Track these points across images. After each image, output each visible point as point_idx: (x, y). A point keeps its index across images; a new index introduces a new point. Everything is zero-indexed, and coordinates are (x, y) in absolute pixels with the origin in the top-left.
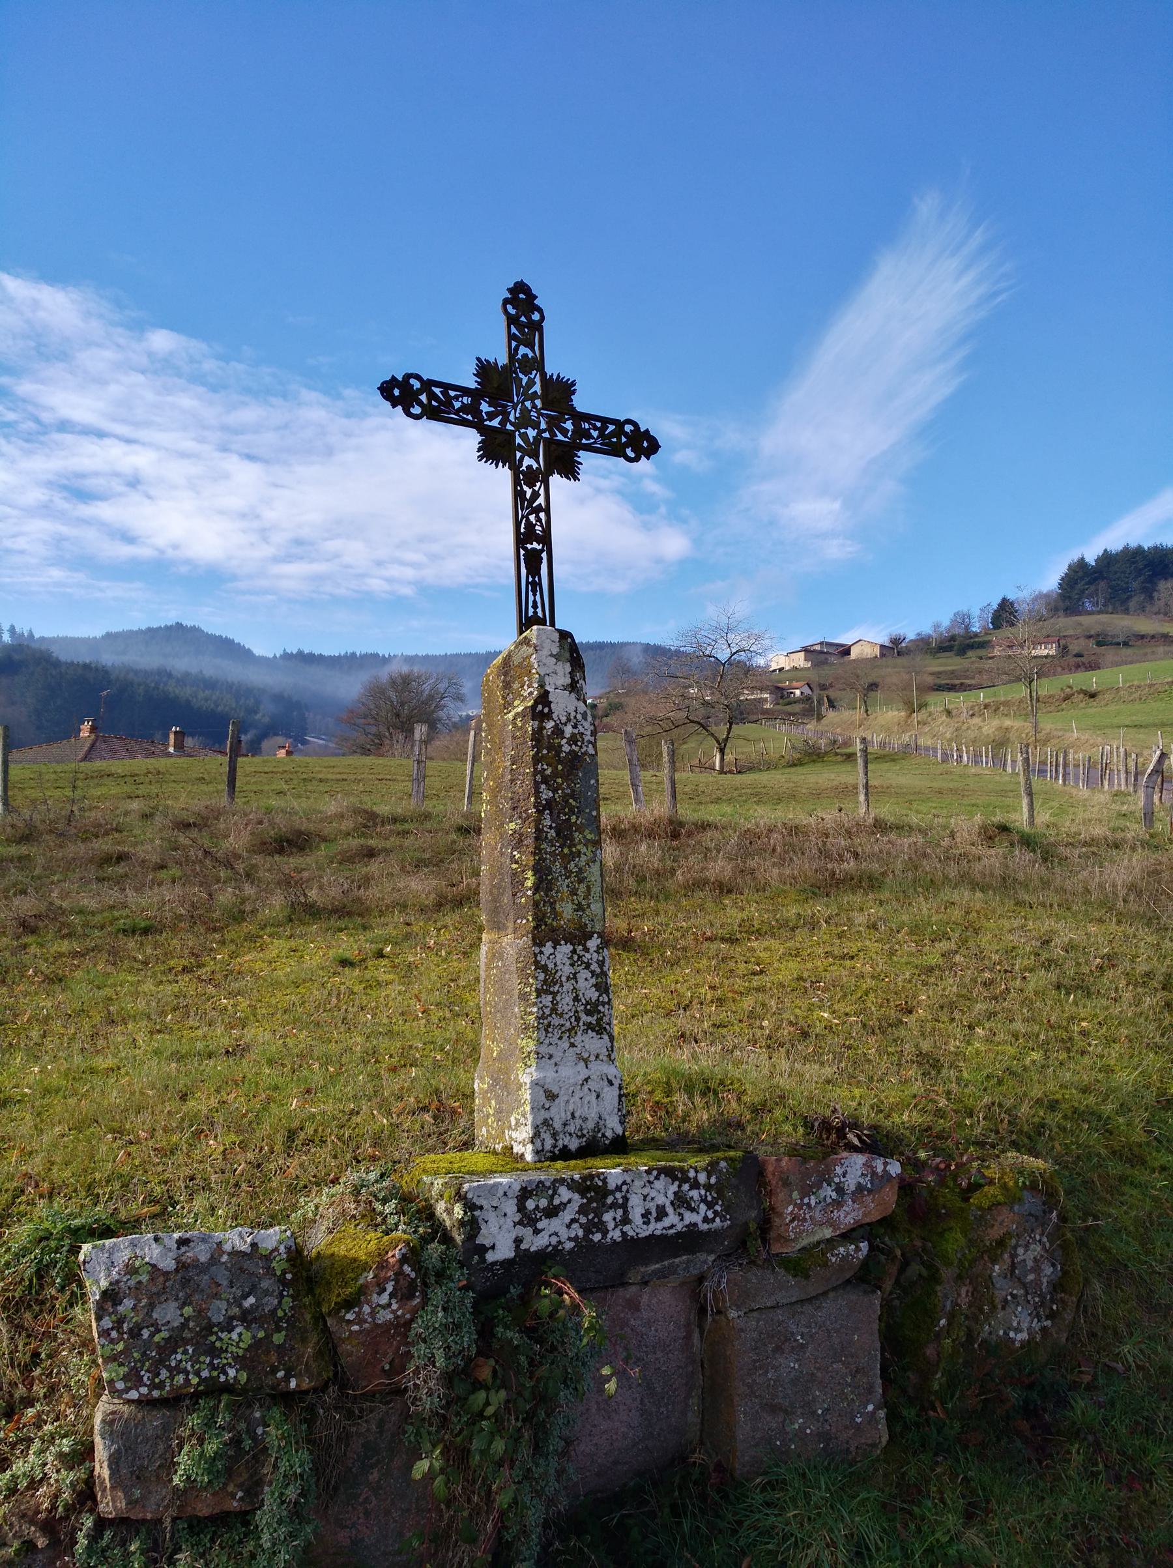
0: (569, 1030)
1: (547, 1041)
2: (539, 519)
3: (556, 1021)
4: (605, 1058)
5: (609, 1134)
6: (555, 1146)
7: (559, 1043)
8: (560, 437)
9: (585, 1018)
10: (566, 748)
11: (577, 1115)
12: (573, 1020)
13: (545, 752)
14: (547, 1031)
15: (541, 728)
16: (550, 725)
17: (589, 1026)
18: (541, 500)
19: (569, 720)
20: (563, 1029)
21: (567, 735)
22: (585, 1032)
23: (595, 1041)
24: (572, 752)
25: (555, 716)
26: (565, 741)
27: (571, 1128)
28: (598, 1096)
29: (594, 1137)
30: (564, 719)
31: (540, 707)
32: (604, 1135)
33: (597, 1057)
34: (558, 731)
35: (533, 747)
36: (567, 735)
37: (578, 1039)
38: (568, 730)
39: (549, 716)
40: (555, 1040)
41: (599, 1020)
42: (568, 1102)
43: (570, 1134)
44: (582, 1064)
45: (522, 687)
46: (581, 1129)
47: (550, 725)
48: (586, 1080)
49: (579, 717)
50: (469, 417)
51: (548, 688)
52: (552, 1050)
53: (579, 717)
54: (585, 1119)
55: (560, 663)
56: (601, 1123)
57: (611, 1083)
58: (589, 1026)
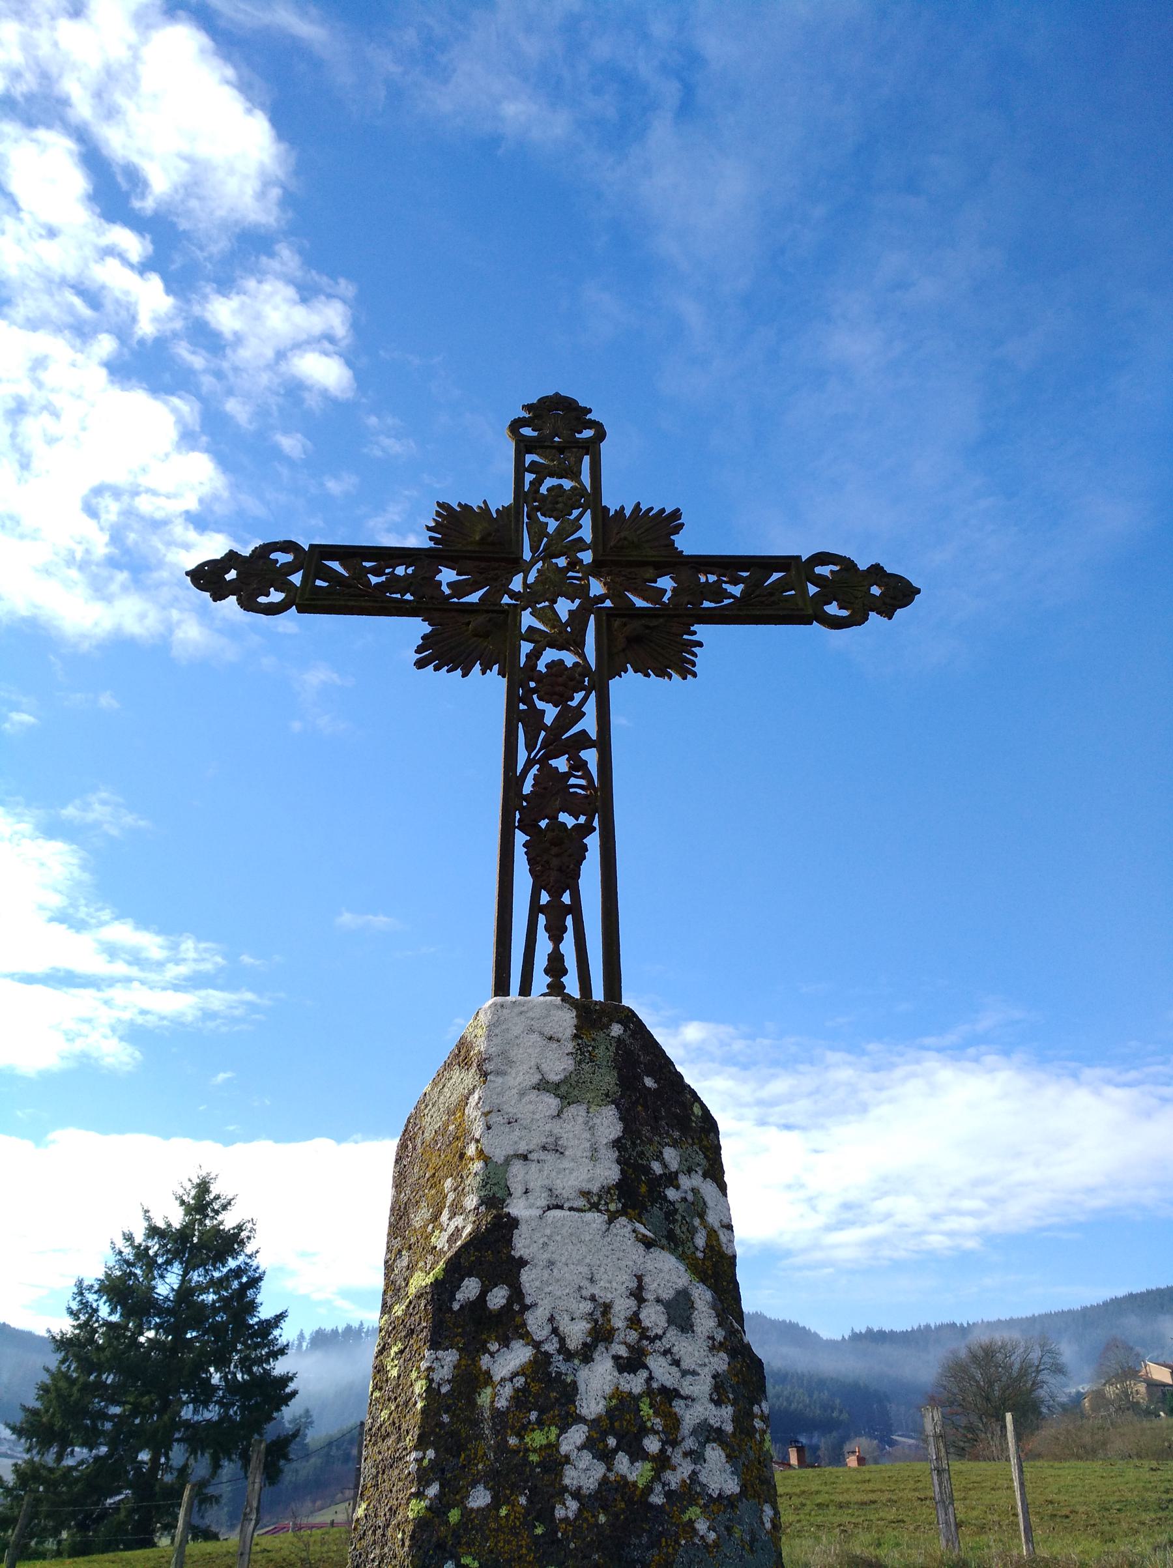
2: (579, 765)
8: (639, 603)
10: (584, 1473)
13: (480, 1498)
15: (471, 1379)
16: (508, 1362)
18: (589, 724)
19: (601, 1334)
21: (592, 1405)
24: (612, 1491)
25: (536, 1322)
26: (577, 1435)
30: (576, 1332)
31: (470, 1288)
34: (548, 1392)
35: (423, 1477)
36: (592, 1405)
38: (597, 1383)
39: (509, 1324)
45: (436, 1217)
47: (508, 1362)
49: (653, 1317)
50: (408, 597)
51: (517, 1208)
53: (653, 1317)
55: (576, 1112)
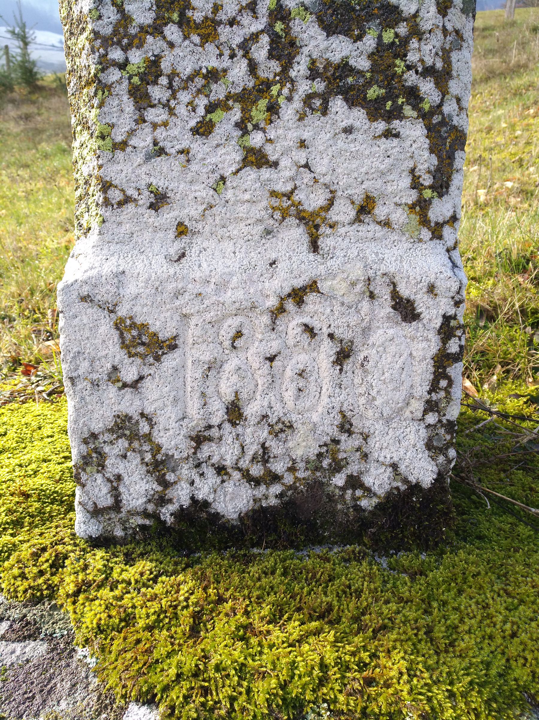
0: (246, 98)
1: (143, 140)
3: (184, 56)
4: (399, 216)
5: (378, 480)
6: (162, 500)
7: (198, 147)
9: (316, 43)
11: (252, 410)
12: (261, 51)
14: (140, 97)
17: (338, 80)
20: (219, 91)
22: (316, 105)
23: (360, 143)
27: (226, 452)
28: (343, 356)
29: (316, 486)
32: (354, 482)
33: (365, 209)
37: (283, 134)
40: (178, 134)
41: (388, 55)
42: (213, 367)
43: (221, 470)
44: (295, 234)
46: (264, 455)
48: (298, 295)
52: (164, 174)
54: (283, 428)
56: (348, 444)
57: (406, 310)
58: (338, 80)
